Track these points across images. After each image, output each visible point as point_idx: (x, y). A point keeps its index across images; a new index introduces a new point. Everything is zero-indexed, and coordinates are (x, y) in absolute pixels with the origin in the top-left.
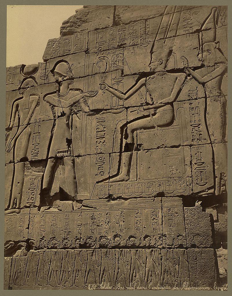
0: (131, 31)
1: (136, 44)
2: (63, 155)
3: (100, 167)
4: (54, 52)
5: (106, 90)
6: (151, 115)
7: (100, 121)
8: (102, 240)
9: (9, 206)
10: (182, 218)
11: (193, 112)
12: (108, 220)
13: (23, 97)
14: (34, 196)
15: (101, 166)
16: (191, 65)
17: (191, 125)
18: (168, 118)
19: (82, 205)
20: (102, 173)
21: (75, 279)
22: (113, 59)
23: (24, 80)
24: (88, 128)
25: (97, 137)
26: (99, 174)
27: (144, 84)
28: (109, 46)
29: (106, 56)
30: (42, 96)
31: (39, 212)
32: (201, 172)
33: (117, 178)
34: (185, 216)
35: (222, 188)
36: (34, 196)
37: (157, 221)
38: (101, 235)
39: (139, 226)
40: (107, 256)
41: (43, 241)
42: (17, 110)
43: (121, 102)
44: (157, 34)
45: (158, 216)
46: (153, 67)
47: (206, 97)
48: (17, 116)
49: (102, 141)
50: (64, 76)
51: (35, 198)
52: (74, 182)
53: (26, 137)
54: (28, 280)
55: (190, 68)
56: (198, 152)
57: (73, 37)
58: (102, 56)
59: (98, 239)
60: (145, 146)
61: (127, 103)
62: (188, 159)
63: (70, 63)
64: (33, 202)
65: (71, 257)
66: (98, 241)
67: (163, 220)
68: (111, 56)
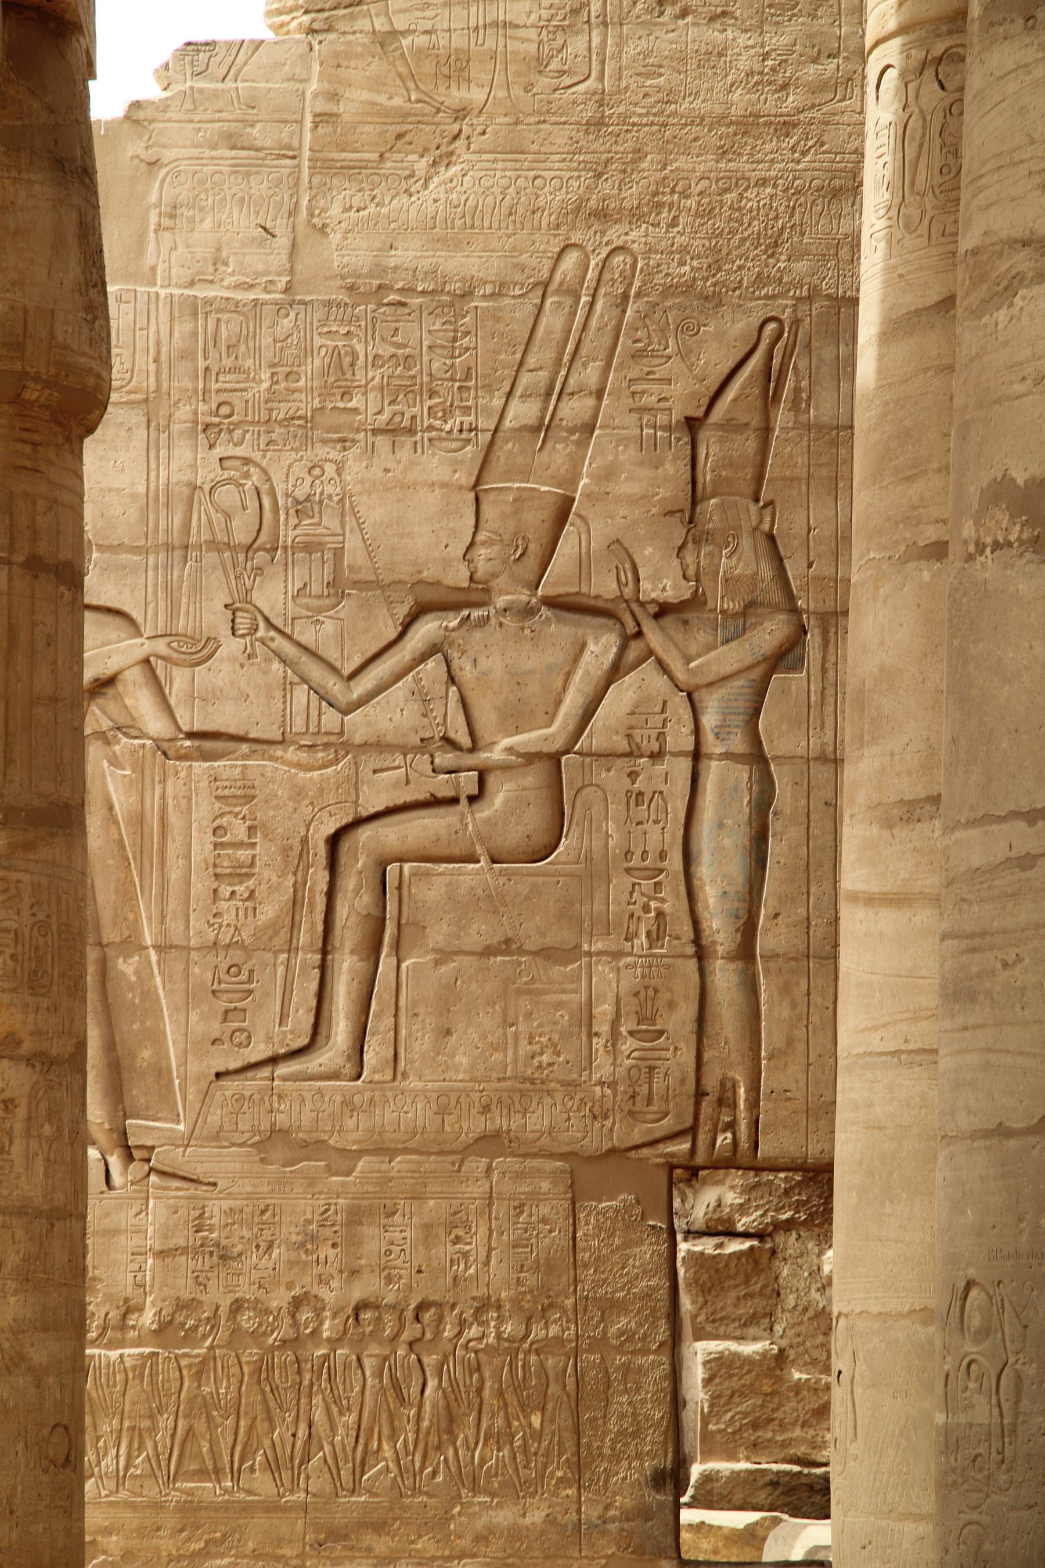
0: (386, 350)
1: (406, 423)
6: (464, 801)
7: (226, 792)
10: (565, 1242)
12: (267, 1235)
16: (649, 590)
17: (628, 870)
19: (151, 1169)
20: (239, 1037)
22: (291, 480)
24: (174, 819)
25: (219, 870)
26: (226, 1037)
28: (275, 405)
29: (256, 456)
33: (312, 1063)
34: (579, 1234)
37: (467, 1248)
39: (398, 1263)
43: (331, 719)
44: (510, 394)
45: (473, 1230)
47: (697, 755)
52: (110, 1065)
55: (642, 604)
56: (646, 988)
58: (239, 451)
59: (223, 1312)
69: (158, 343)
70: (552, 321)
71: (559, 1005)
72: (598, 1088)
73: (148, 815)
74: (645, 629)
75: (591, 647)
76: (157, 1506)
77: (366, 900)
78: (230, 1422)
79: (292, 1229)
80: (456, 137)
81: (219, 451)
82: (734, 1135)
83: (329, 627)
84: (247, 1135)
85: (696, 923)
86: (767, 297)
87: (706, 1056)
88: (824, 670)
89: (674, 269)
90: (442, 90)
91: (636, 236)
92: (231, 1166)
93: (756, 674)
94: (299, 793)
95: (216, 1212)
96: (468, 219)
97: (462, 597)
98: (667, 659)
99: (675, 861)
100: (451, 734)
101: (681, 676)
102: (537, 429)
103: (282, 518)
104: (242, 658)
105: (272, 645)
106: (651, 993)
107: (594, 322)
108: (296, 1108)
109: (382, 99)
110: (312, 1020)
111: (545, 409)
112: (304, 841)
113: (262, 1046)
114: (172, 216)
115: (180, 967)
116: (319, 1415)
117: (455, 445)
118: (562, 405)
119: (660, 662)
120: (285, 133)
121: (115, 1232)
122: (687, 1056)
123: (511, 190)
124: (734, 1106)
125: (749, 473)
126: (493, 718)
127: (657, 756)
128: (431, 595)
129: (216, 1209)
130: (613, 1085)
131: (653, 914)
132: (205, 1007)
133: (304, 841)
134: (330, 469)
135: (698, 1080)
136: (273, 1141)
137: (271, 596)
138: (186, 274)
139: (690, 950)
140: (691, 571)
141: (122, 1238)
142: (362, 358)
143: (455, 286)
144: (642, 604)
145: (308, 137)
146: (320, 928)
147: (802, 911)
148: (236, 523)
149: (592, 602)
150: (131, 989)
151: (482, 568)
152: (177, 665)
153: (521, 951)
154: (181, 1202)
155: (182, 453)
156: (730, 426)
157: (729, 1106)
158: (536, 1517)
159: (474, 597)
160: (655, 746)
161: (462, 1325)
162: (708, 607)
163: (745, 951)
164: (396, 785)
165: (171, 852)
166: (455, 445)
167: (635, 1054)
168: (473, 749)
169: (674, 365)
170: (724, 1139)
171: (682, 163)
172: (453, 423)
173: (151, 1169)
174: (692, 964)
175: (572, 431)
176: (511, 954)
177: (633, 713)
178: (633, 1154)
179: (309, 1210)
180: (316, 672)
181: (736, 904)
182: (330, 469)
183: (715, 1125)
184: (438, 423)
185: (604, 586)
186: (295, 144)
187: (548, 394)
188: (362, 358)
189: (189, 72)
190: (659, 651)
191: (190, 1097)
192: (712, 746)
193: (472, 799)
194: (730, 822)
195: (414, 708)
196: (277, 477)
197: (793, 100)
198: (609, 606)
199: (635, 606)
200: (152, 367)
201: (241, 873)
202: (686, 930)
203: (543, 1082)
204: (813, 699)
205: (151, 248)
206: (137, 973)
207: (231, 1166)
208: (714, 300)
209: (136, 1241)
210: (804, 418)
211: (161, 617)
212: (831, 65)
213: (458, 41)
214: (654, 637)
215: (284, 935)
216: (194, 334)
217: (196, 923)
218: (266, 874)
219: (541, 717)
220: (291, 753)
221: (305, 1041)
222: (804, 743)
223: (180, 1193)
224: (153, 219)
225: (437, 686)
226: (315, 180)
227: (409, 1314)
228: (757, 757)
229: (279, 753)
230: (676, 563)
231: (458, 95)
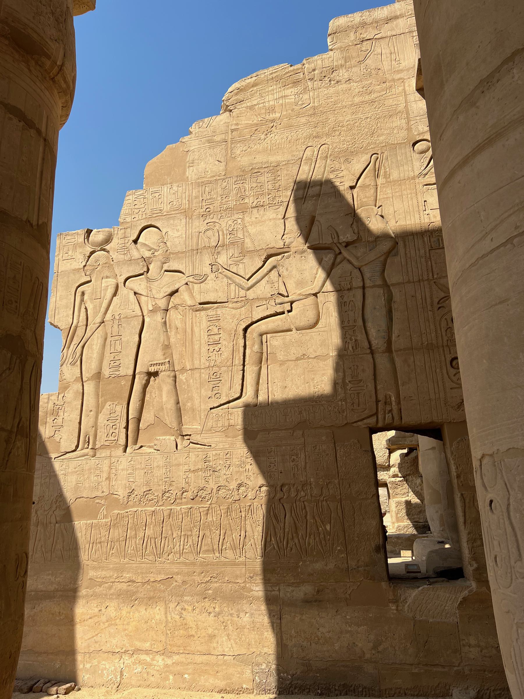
0: (254, 185)
1: (261, 204)
2: (159, 369)
3: (215, 386)
5: (220, 273)
6: (286, 312)
7: (211, 319)
8: (220, 492)
9: (77, 446)
13: (90, 281)
15: (217, 385)
16: (343, 239)
18: (311, 316)
19: (190, 442)
20: (218, 395)
21: (183, 550)
23: (92, 253)
25: (209, 343)
27: (274, 267)
29: (217, 221)
30: (121, 280)
31: (124, 453)
32: (358, 393)
34: (338, 455)
35: (387, 416)
36: (117, 430)
38: (219, 485)
39: (274, 470)
40: (229, 514)
41: (133, 496)
42: (82, 300)
43: (242, 293)
45: (299, 456)
46: (287, 241)
47: (364, 288)
48: (83, 310)
49: (217, 349)
50: (154, 249)
51: (117, 433)
52: (177, 409)
53: (99, 342)
54: (112, 553)
55: (340, 244)
57: (165, 190)
60: (281, 356)
61: (251, 294)
63: (164, 231)
64: (113, 439)
65: (175, 517)
66: (215, 494)
67: (307, 461)
68: (226, 221)
69: (189, 196)
71: (323, 375)
72: (340, 403)
73: (188, 330)
74: (342, 251)
75: (325, 259)
76: (193, 564)
77: (256, 347)
78: (218, 532)
79: (237, 460)
80: (272, 127)
81: (206, 222)
82: (392, 414)
83: (241, 266)
84: (221, 428)
85: (369, 343)
86: (372, 148)
87: (378, 387)
88: (406, 254)
89: (341, 146)
90: (267, 116)
91: (328, 141)
92: (216, 440)
93: (382, 259)
94: (234, 316)
95: (211, 456)
96: (277, 146)
97: (282, 250)
98: (351, 259)
99: (360, 322)
100: (281, 292)
101: (356, 263)
102: (302, 198)
103: (225, 236)
104: (215, 279)
105: (224, 273)
106: (356, 367)
107: (317, 165)
108: (236, 418)
109: (251, 122)
110: (240, 388)
111: (304, 192)
112: (236, 331)
113: (224, 398)
114: (192, 163)
115: (198, 375)
116: (248, 528)
117: (277, 207)
118: (310, 190)
119: (348, 260)
120: (223, 136)
121: (179, 465)
122: (371, 386)
123: (290, 137)
124: (391, 404)
125: (373, 198)
126: (294, 285)
127: (350, 289)
128: (272, 251)
129: (211, 454)
130: (345, 400)
131: (354, 340)
132: (206, 387)
133: (236, 331)
134: (239, 221)
135: (376, 396)
137: (222, 259)
138: (197, 177)
139: (368, 351)
140: (356, 231)
141: (181, 467)
142: (247, 188)
143: (275, 164)
144: (340, 244)
145: (230, 136)
146: (242, 357)
147: (408, 333)
148: (212, 240)
149: (324, 246)
150: (184, 384)
151: (287, 241)
152: (196, 283)
153: (309, 358)
154: (201, 453)
155: (196, 223)
156: (364, 187)
157: (389, 404)
158: (331, 566)
159: (285, 250)
160: (349, 287)
161: (297, 491)
162: (363, 240)
163: (389, 349)
164: (264, 310)
165: (194, 339)
166: (277, 207)
167: (352, 389)
168: (288, 296)
169: (344, 173)
170: (388, 416)
171: (341, 118)
172: (276, 202)
173: (190, 442)
174: (370, 356)
175: (313, 196)
176: (305, 359)
177: (340, 277)
178: (355, 425)
179: (242, 452)
180: (237, 279)
181: (384, 334)
182: (239, 221)
183: (385, 412)
184: (271, 202)
186: (227, 138)
187: (305, 188)
188: (247, 188)
189: (197, 128)
190: (348, 257)
191: (202, 417)
192: (368, 283)
193: (289, 311)
194: (378, 307)
195: (268, 286)
196: (224, 225)
197: (373, 96)
198: (330, 246)
199: (338, 245)
200: (187, 202)
201: (217, 343)
202: (366, 344)
203: (320, 402)
204: (403, 263)
205: (187, 173)
206: (186, 379)
207: (216, 440)
208: (354, 153)
209: (186, 467)
210: (389, 180)
211: (191, 270)
212: (384, 85)
213: (271, 103)
214: (345, 253)
215: (230, 361)
216: (199, 191)
217: (203, 360)
218: (224, 343)
219: (310, 283)
220: (231, 305)
221: (238, 395)
222: (402, 278)
223: (199, 450)
224: (188, 165)
225: (275, 278)
226: (233, 146)
227: (278, 489)
228: (386, 285)
229: (227, 305)
230: (351, 229)
231: (272, 116)
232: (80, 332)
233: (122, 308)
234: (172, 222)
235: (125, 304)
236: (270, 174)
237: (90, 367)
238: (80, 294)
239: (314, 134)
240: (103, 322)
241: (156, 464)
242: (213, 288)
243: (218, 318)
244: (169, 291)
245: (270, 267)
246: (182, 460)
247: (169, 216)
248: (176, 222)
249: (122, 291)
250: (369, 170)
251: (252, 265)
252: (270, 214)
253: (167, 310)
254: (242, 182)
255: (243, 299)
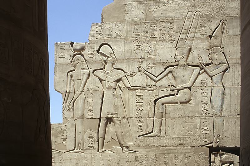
4: (98, 35)
6: (175, 95)
7: (138, 95)
11: (204, 95)
12: (146, 159)
13: (75, 70)
14: (93, 143)
15: (141, 126)
22: (147, 48)
23: (74, 55)
27: (170, 72)
30: (91, 70)
43: (154, 83)
44: (181, 33)
58: (139, 45)
62: (198, 125)
70: (187, 23)
121: (124, 159)
123: (180, 4)
136: (147, 146)
137: (144, 65)
141: (125, 160)
152: (130, 76)
185: (197, 61)
232: (71, 95)
233: (92, 85)
234: (117, 43)
235: (93, 83)
236: (169, 23)
237: (78, 113)
238: (70, 76)
239: (193, 5)
240: (83, 92)
241: (113, 158)
242: (140, 80)
243: (142, 95)
244: (116, 79)
245: (168, 72)
246: (125, 156)
247: (116, 41)
248: (119, 43)
249: (92, 76)
250: (219, 28)
251: (159, 70)
252: (169, 45)
253: (116, 88)
254: (154, 26)
255: (154, 86)
